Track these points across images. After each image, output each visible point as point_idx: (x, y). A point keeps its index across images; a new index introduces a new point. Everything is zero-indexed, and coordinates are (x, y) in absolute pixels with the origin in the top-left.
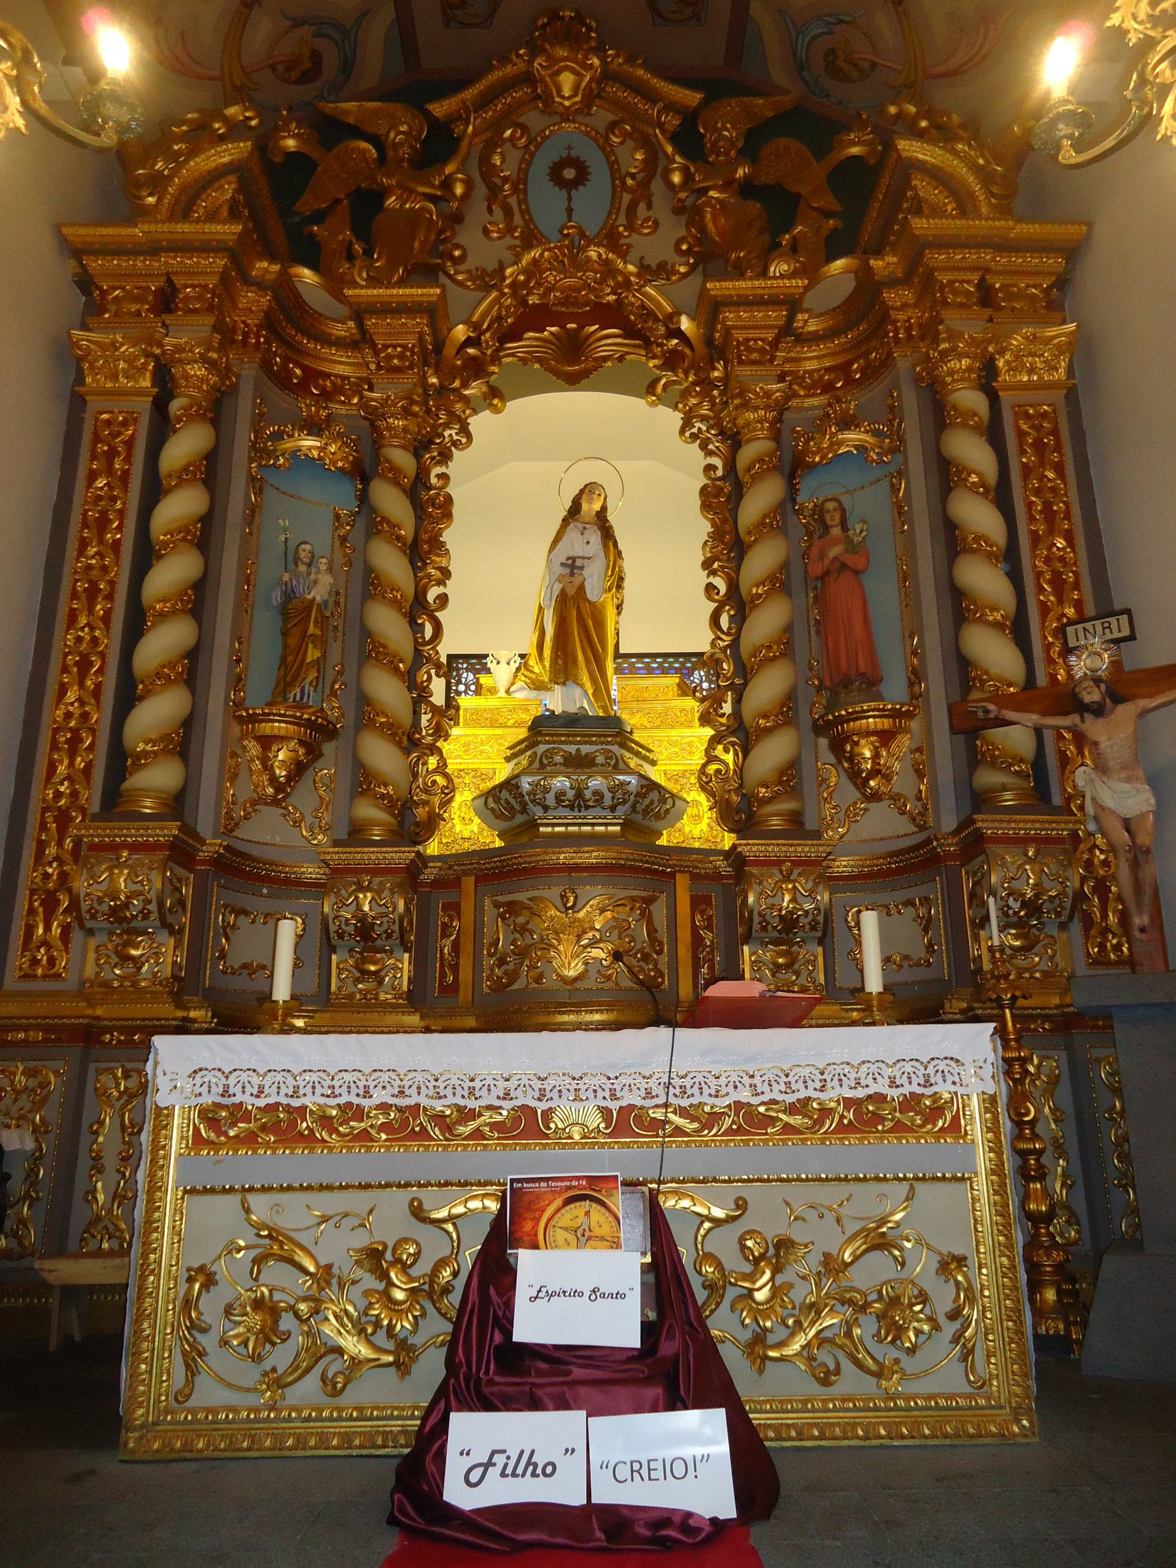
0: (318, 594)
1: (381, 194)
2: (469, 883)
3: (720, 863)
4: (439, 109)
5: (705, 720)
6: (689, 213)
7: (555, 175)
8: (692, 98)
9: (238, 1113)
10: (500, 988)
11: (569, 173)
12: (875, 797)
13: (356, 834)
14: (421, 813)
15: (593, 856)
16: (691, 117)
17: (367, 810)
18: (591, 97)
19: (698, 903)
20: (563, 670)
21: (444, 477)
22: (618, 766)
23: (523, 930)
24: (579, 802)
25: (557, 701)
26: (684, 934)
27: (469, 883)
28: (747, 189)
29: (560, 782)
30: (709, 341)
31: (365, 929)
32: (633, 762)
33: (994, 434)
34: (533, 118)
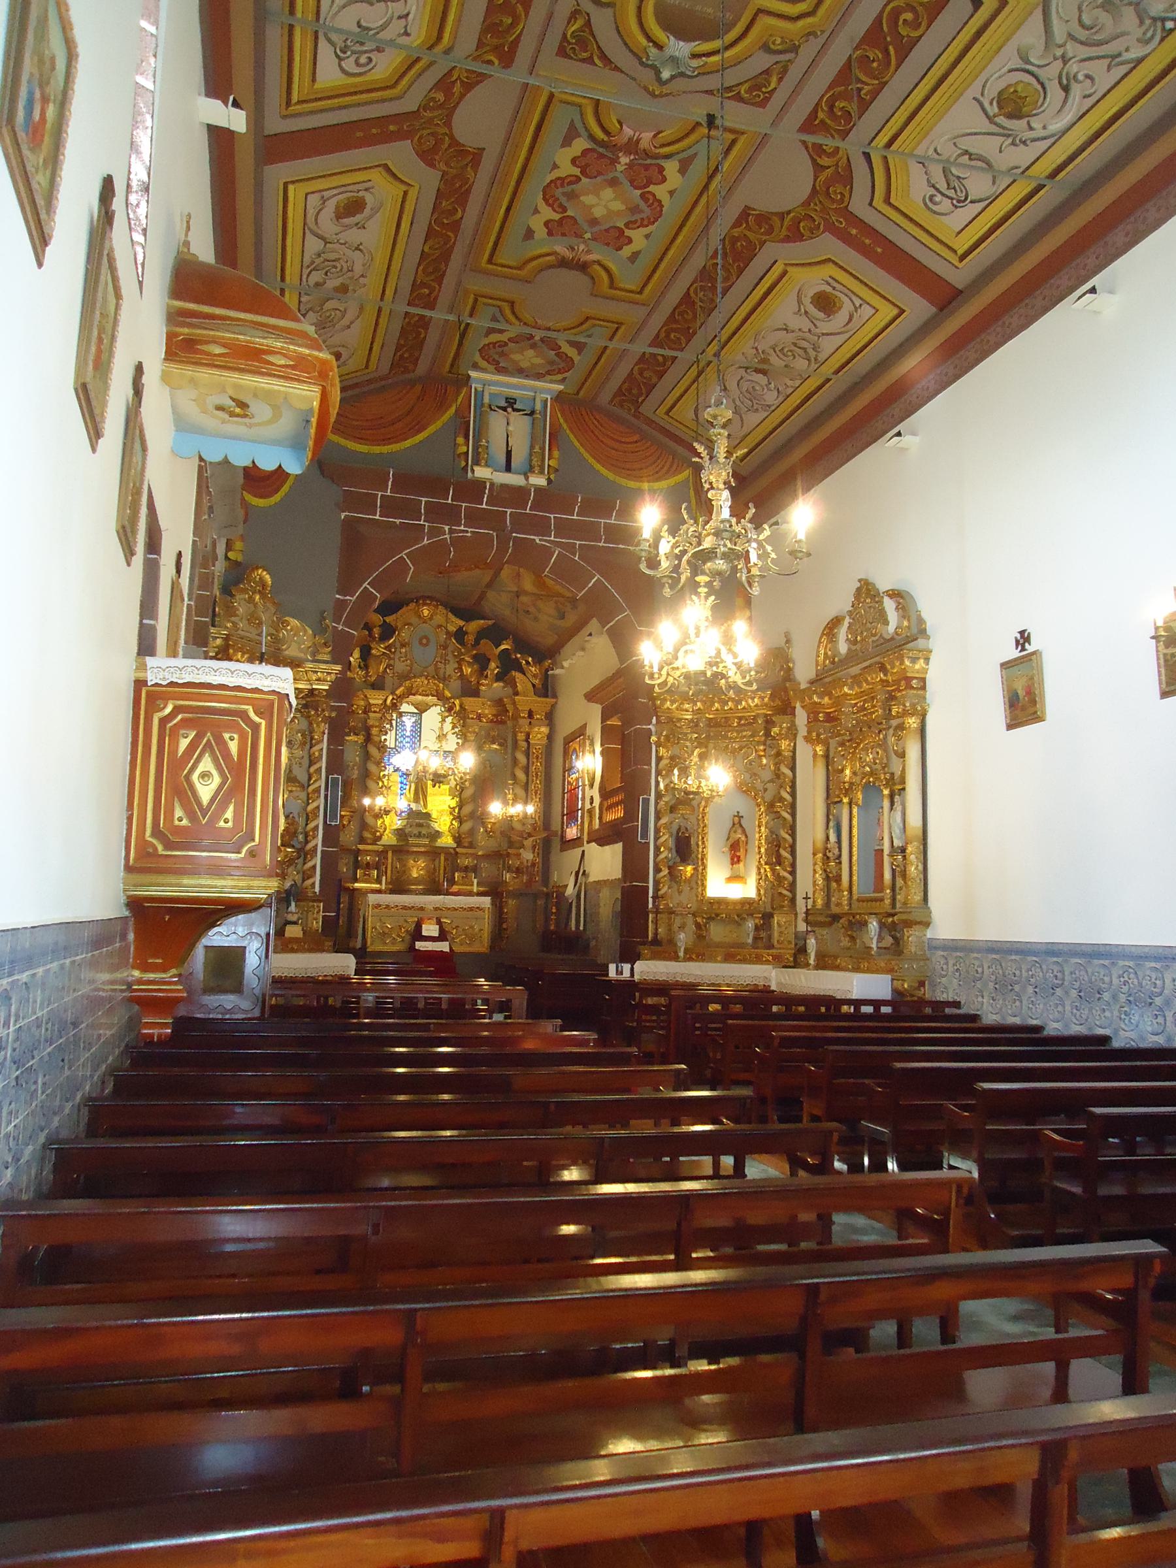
0: (355, 777)
1: (370, 648)
2: (390, 854)
3: (452, 851)
4: (388, 619)
5: (451, 813)
6: (460, 662)
7: (421, 643)
8: (461, 623)
9: (380, 906)
10: (397, 879)
11: (424, 641)
12: (491, 836)
13: (362, 840)
14: (378, 834)
15: (423, 849)
16: (461, 628)
17: (367, 835)
18: (431, 619)
19: (446, 860)
20: (416, 800)
21: (385, 740)
22: (429, 826)
23: (405, 865)
24: (419, 835)
25: (414, 806)
26: (442, 868)
27: (390, 854)
28: (475, 657)
29: (416, 832)
30: (461, 706)
31: (368, 864)
32: (432, 824)
33: (527, 754)
34: (414, 620)
